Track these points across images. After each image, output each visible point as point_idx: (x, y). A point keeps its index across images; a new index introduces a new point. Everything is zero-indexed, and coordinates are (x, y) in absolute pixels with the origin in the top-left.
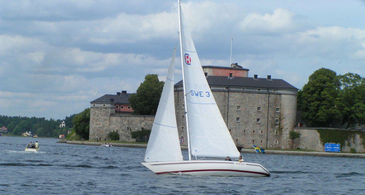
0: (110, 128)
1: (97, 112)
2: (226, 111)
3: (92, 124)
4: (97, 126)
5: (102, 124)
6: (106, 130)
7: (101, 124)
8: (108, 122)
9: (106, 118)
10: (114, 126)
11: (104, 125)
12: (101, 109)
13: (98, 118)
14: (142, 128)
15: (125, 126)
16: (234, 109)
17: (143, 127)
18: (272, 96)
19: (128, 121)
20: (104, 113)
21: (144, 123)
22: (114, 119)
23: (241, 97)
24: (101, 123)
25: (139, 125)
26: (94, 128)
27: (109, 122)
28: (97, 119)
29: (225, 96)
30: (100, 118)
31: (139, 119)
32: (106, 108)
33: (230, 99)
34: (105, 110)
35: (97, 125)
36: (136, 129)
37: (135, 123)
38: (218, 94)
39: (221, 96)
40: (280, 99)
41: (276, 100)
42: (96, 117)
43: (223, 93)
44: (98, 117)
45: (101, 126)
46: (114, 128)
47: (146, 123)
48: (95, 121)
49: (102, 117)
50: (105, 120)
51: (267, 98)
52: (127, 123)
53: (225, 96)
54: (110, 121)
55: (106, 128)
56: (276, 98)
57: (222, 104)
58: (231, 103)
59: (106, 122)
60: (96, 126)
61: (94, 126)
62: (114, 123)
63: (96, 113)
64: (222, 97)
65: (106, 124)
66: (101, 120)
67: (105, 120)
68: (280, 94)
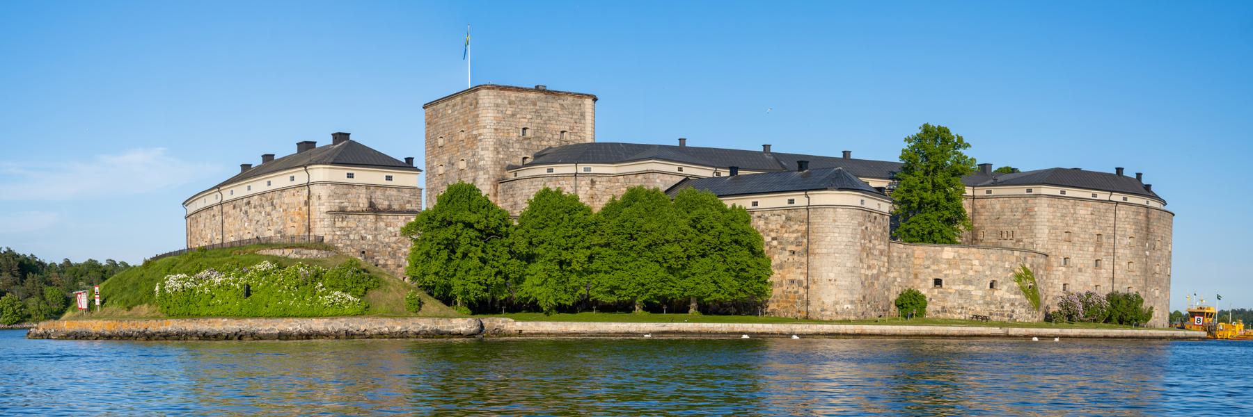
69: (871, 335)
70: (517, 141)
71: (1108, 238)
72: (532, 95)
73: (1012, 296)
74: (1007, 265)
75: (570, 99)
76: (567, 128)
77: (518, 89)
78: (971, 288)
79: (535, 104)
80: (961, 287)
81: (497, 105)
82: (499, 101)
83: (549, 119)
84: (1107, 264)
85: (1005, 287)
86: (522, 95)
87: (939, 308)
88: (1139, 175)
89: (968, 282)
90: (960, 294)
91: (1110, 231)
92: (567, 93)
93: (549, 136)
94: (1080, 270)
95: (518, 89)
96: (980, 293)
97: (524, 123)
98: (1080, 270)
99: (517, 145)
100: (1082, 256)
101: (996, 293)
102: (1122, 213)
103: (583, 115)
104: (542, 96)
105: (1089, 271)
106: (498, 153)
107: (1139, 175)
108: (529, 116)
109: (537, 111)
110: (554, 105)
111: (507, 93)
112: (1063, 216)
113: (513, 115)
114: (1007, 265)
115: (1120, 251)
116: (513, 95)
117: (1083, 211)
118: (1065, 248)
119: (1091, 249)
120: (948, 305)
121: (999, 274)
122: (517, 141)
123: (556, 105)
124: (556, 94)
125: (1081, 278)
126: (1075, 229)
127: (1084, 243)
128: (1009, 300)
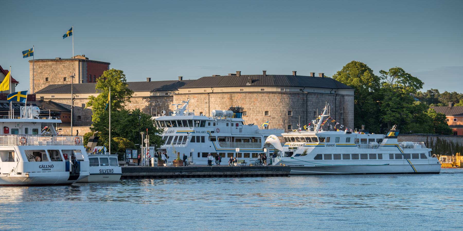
2: (305, 118)
16: (312, 115)
18: (338, 98)
23: (317, 101)
29: (304, 100)
33: (309, 103)
38: (297, 98)
39: (300, 100)
40: (344, 100)
41: (340, 102)
43: (301, 96)
51: (334, 102)
53: (304, 100)
56: (340, 101)
57: (301, 110)
58: (310, 109)
64: (301, 102)
68: (343, 96)
72: (50, 63)
75: (68, 62)
76: (66, 76)
86: (45, 63)
88: (264, 72)
91: (207, 110)
93: (58, 80)
102: (213, 98)
104: (55, 63)
107: (264, 72)
108: (48, 72)
109: (52, 70)
110: (60, 66)
113: (41, 73)
116: (41, 64)
117: (193, 101)
123: (61, 66)
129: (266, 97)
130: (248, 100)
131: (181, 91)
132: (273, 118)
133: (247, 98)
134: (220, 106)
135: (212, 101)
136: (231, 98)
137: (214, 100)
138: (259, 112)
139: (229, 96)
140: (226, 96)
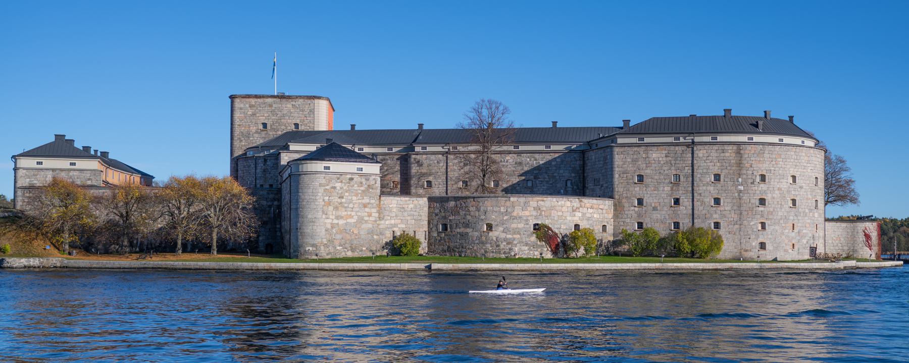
0: (381, 226)
1: (338, 185)
3: (324, 216)
4: (341, 222)
5: (356, 217)
6: (371, 232)
7: (351, 217)
8: (374, 210)
9: (366, 200)
10: (393, 222)
11: (361, 220)
12: (351, 179)
13: (343, 200)
14: (577, 226)
15: (527, 220)
17: (579, 222)
19: (538, 209)
20: (362, 188)
21: (580, 214)
22: (394, 202)
24: (353, 214)
25: (569, 218)
26: (329, 226)
27: (379, 212)
28: (341, 203)
30: (351, 202)
31: (568, 204)
32: (367, 176)
34: (363, 180)
35: (337, 218)
36: (563, 227)
37: (560, 214)
42: (336, 200)
44: (342, 197)
45: (349, 220)
46: (395, 225)
47: (584, 214)
48: (331, 208)
49: (354, 198)
50: (365, 206)
52: (534, 213)
54: (379, 205)
55: (370, 226)
59: (367, 210)
60: (336, 221)
61: (329, 221)
62: (394, 214)
63: (334, 188)
65: (370, 215)
66: (351, 205)
67: (365, 206)
69: (348, 270)
70: (256, 132)
71: (686, 176)
72: (269, 100)
73: (509, 236)
74: (502, 209)
76: (298, 121)
77: (256, 97)
78: (469, 230)
79: (271, 106)
80: (462, 230)
81: (241, 109)
82: (242, 106)
83: (284, 116)
84: (686, 202)
85: (501, 229)
87: (446, 248)
89: (467, 225)
90: (462, 235)
91: (690, 171)
92: (297, 97)
94: (655, 209)
95: (256, 97)
96: (476, 234)
97: (262, 119)
98: (655, 209)
99: (256, 135)
100: (658, 196)
101: (491, 234)
103: (312, 111)
104: (278, 100)
105: (665, 209)
106: (241, 141)
110: (288, 105)
111: (247, 100)
112: (635, 161)
113: (254, 114)
114: (502, 209)
115: (700, 189)
116: (253, 101)
117: (656, 155)
118: (638, 190)
119: (667, 189)
120: (452, 245)
121: (493, 218)
122: (256, 132)
123: (289, 106)
124: (289, 97)
125: (656, 215)
126: (648, 171)
127: (659, 183)
128: (505, 240)
129: (792, 152)
130: (766, 155)
131: (620, 141)
132: (801, 187)
133: (766, 152)
134: (718, 164)
135: (701, 155)
136: (738, 153)
137: (706, 155)
138: (783, 177)
139: (735, 147)
140: (730, 147)
